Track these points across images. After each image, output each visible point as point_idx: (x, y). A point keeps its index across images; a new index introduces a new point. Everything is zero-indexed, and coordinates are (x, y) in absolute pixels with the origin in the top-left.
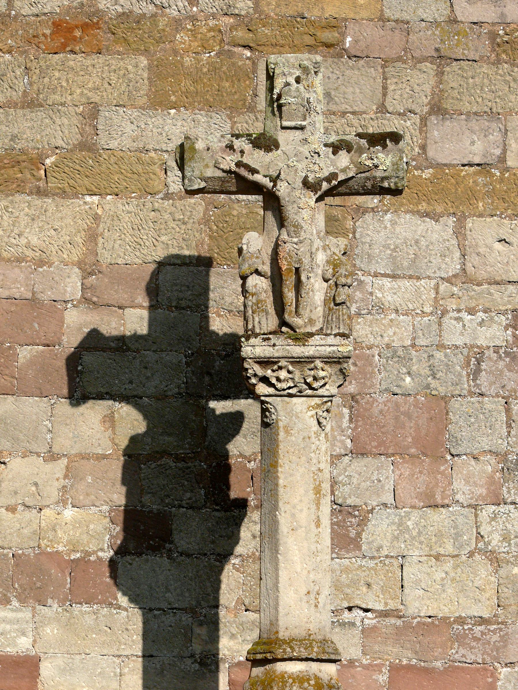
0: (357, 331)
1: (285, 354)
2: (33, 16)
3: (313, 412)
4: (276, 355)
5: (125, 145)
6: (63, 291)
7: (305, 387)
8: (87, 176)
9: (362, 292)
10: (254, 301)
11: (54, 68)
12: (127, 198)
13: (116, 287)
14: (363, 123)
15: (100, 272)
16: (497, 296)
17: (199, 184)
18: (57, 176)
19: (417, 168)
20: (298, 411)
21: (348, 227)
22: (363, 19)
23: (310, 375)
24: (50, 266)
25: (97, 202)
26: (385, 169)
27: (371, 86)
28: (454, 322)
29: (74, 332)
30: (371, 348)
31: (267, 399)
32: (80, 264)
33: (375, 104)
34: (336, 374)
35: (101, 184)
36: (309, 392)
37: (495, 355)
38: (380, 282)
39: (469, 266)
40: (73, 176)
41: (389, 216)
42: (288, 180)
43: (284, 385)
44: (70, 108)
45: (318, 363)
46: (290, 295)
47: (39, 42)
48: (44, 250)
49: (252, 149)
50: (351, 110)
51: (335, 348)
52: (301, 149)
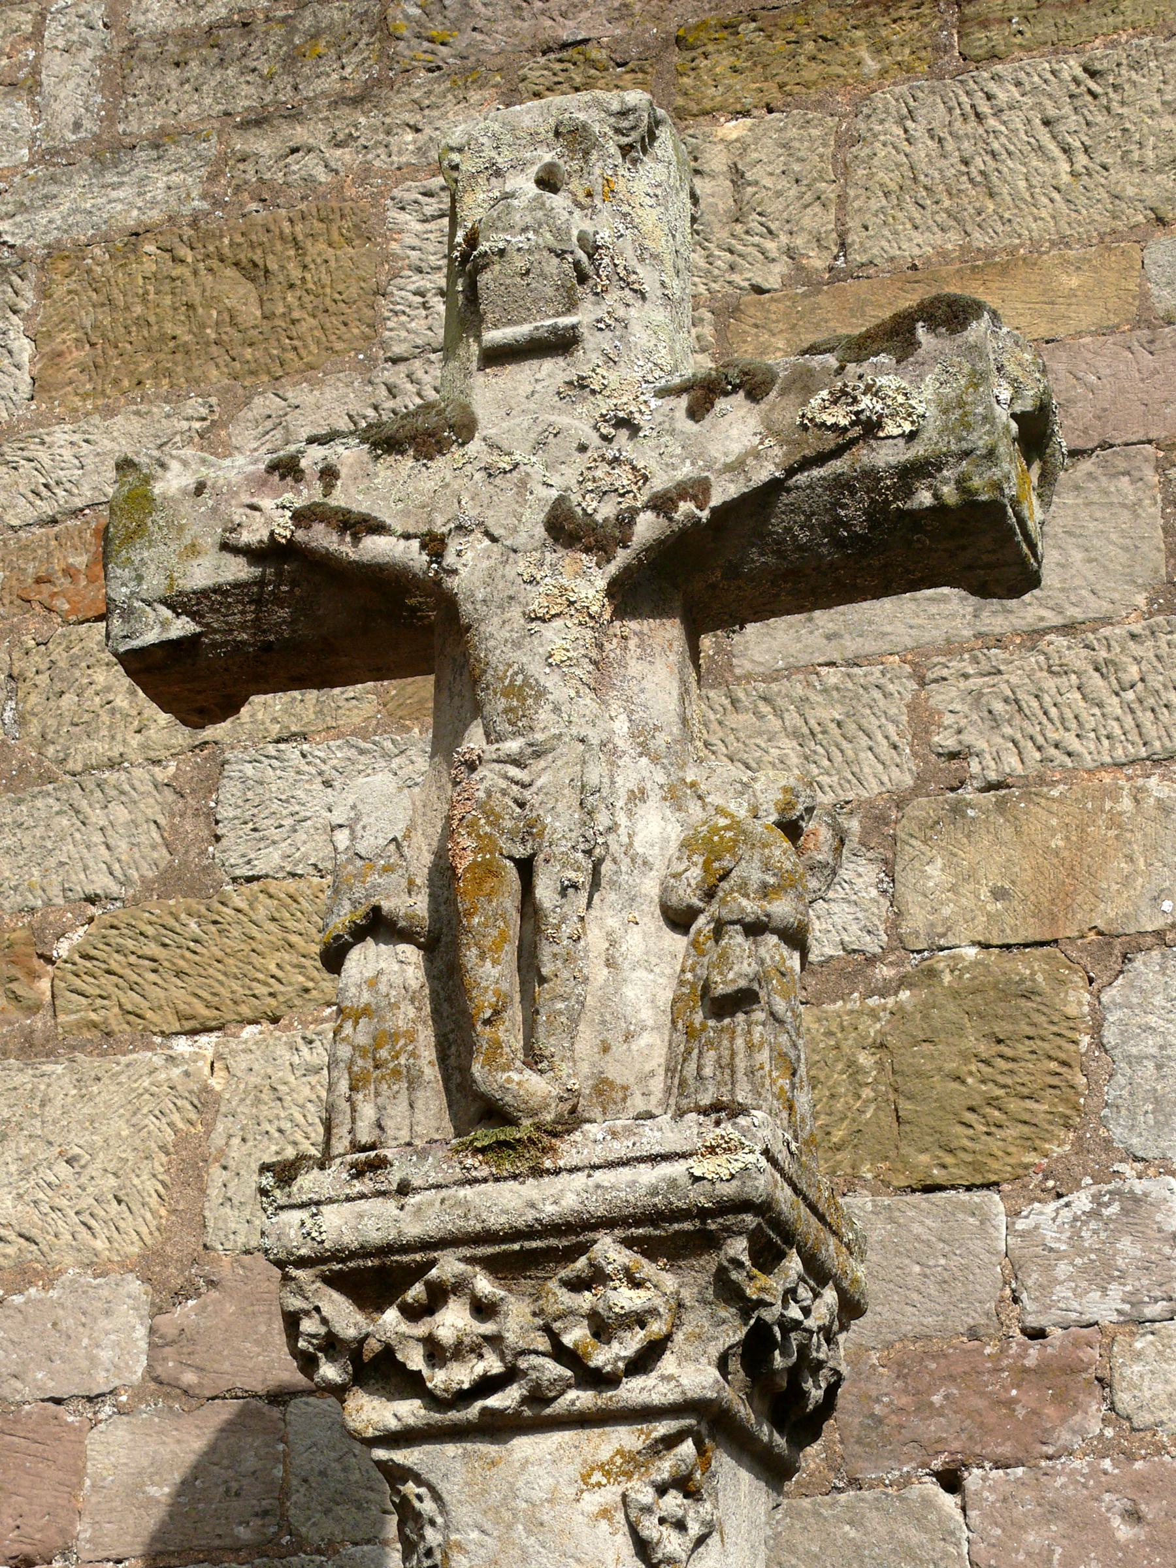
0: (1133, 1386)
1: (452, 1223)
2: (42, 523)
3: (610, 1494)
4: (413, 1230)
5: (306, 856)
6: (84, 1364)
7: (554, 1369)
8: (179, 974)
9: (1139, 1236)
10: (362, 1039)
11: (92, 660)
12: (305, 1024)
13: (263, 1329)
14: (1104, 654)
15: (211, 1283)
17: (165, 624)
18: (84, 987)
20: (538, 1495)
21: (1071, 1010)
22: (1079, 334)
23: (572, 1312)
24: (48, 1286)
25: (209, 1054)
26: (908, 427)
27: (1123, 534)
29: (117, 1503)
31: (401, 1456)
32: (147, 1266)
33: (1144, 587)
34: (704, 1302)
35: (222, 991)
36: (582, 1399)
40: (135, 978)
42: (491, 523)
43: (462, 1375)
44: (138, 772)
45: (609, 1250)
46: (491, 974)
47: (53, 595)
48: (34, 1233)
49: (366, 458)
50: (1058, 621)
51: (677, 1169)
52: (562, 420)
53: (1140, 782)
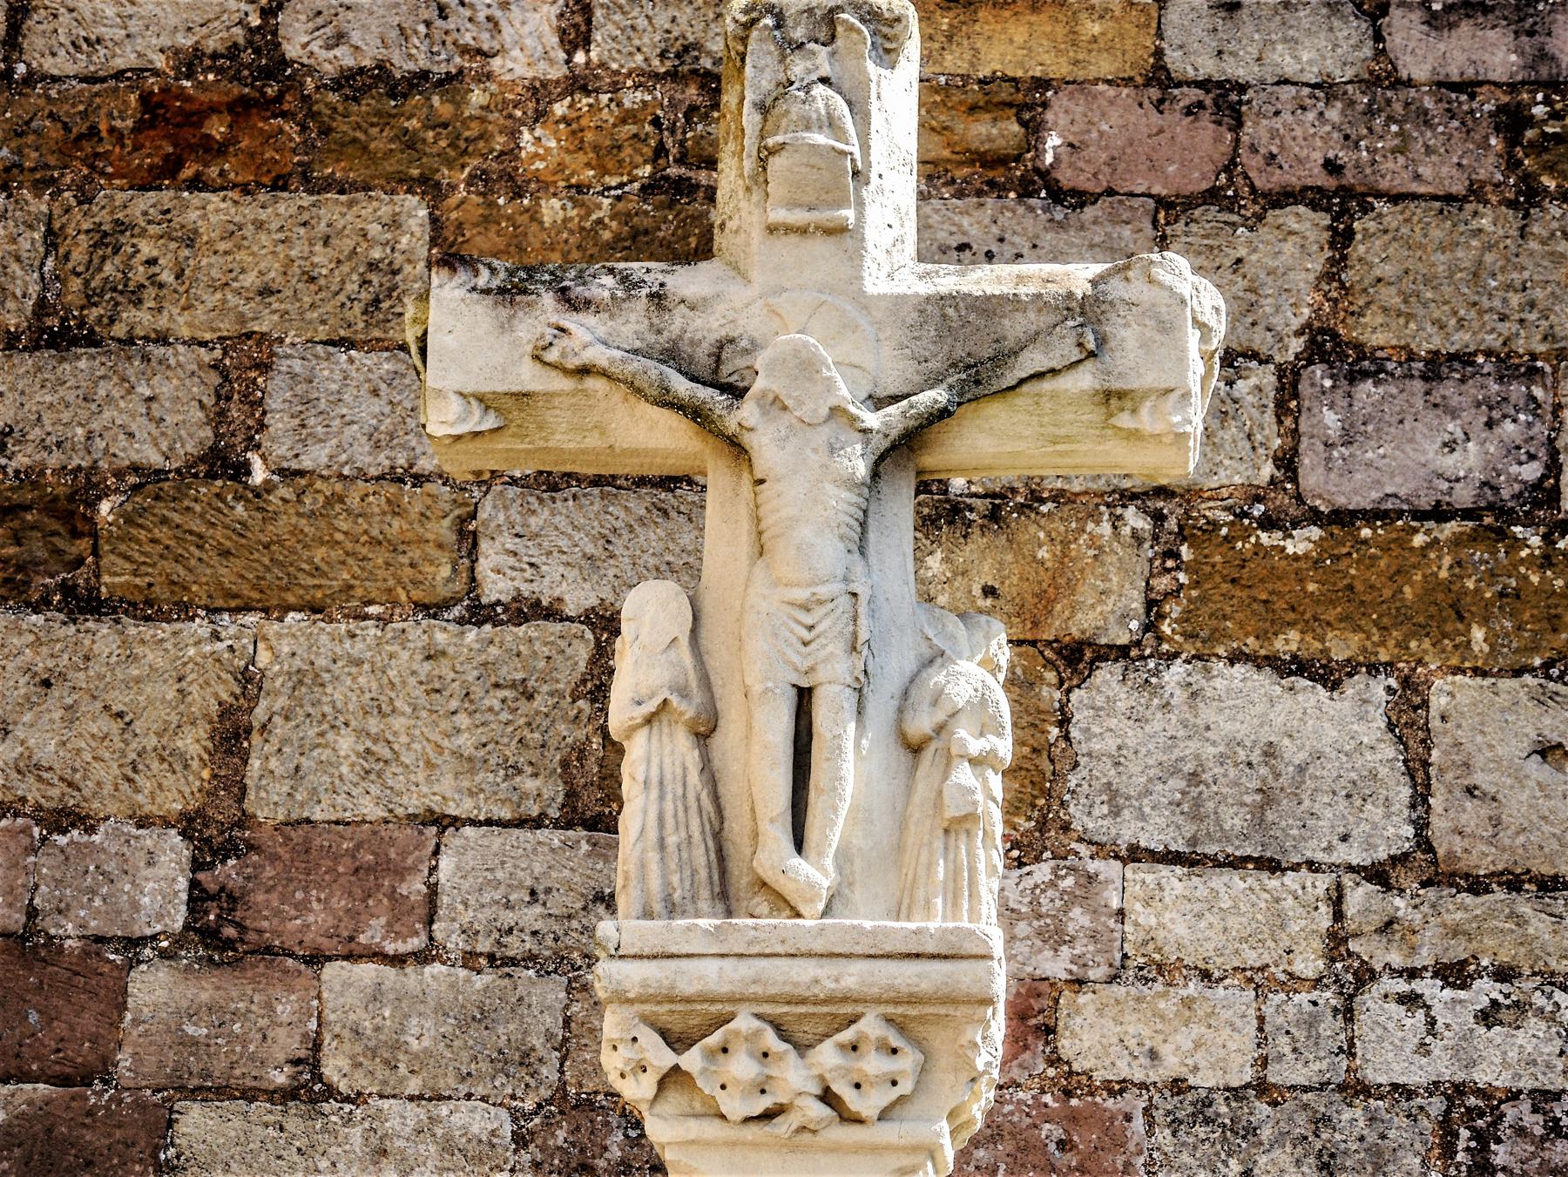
16: (1539, 925)
19: (1268, 523)
24: (90, 830)
28: (1398, 1011)
30: (1121, 1092)
32: (188, 825)
37: (1540, 1118)
38: (1149, 878)
39: (1439, 826)
41: (1178, 669)
53: (1119, 511)
